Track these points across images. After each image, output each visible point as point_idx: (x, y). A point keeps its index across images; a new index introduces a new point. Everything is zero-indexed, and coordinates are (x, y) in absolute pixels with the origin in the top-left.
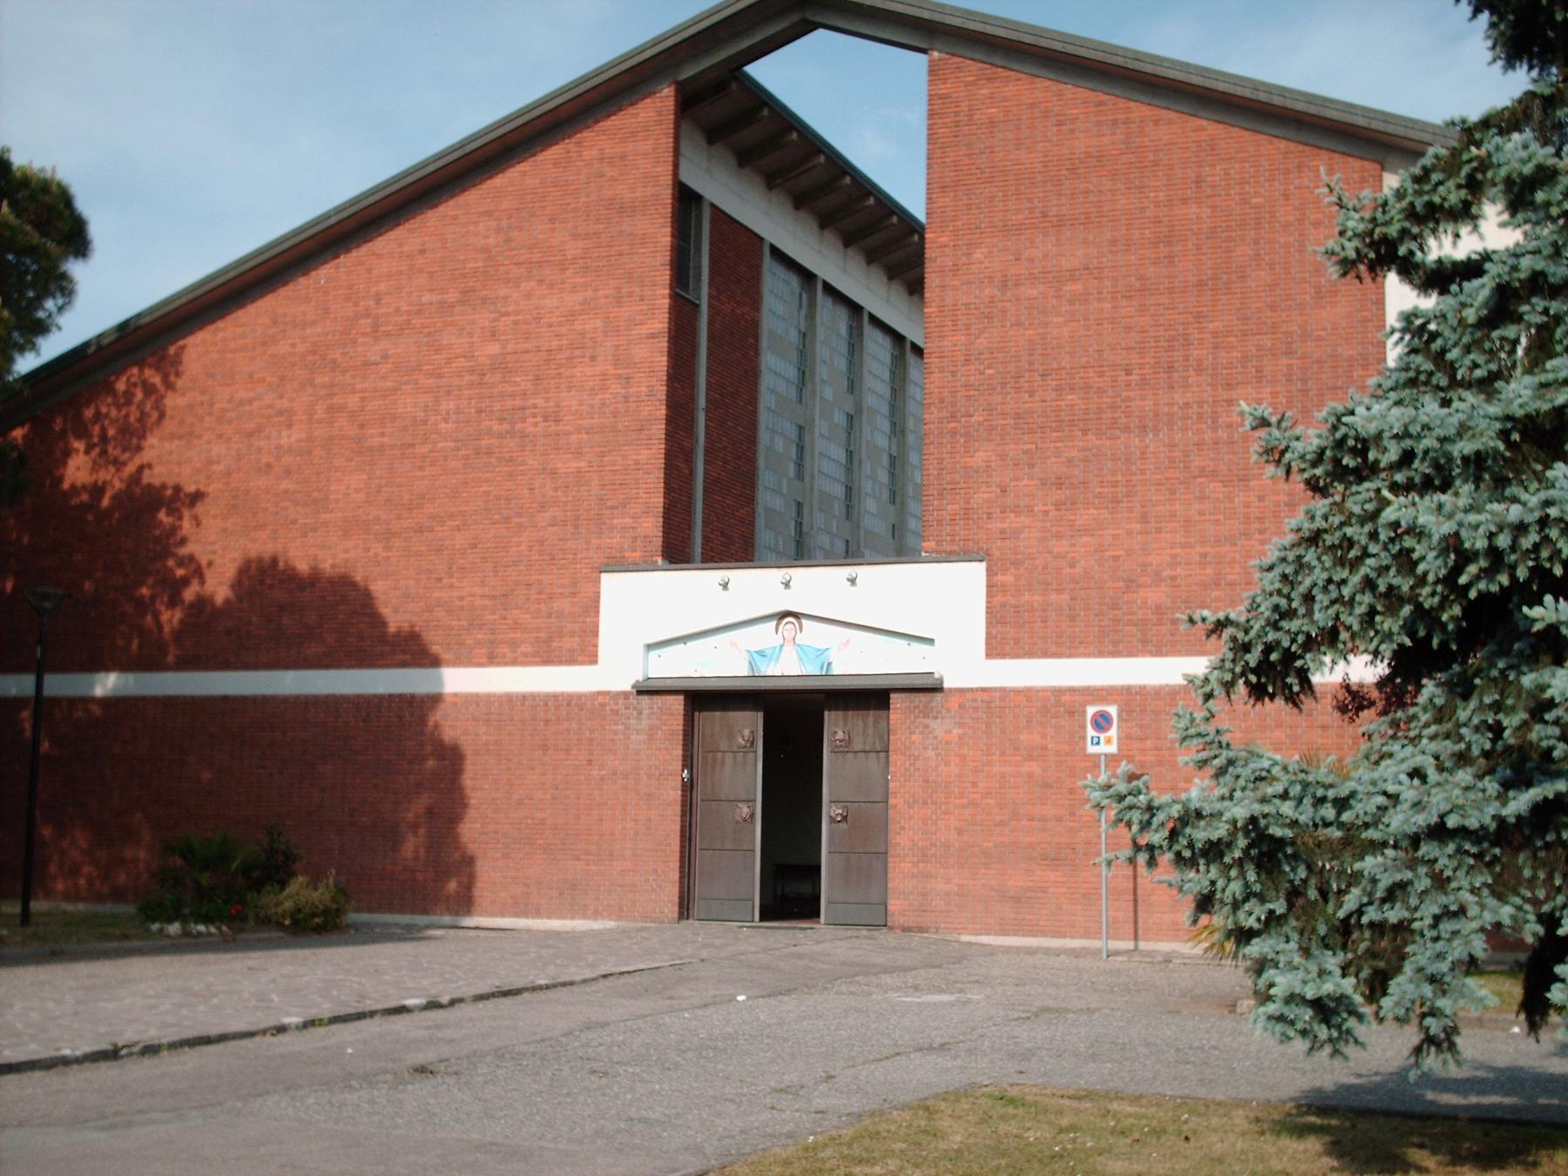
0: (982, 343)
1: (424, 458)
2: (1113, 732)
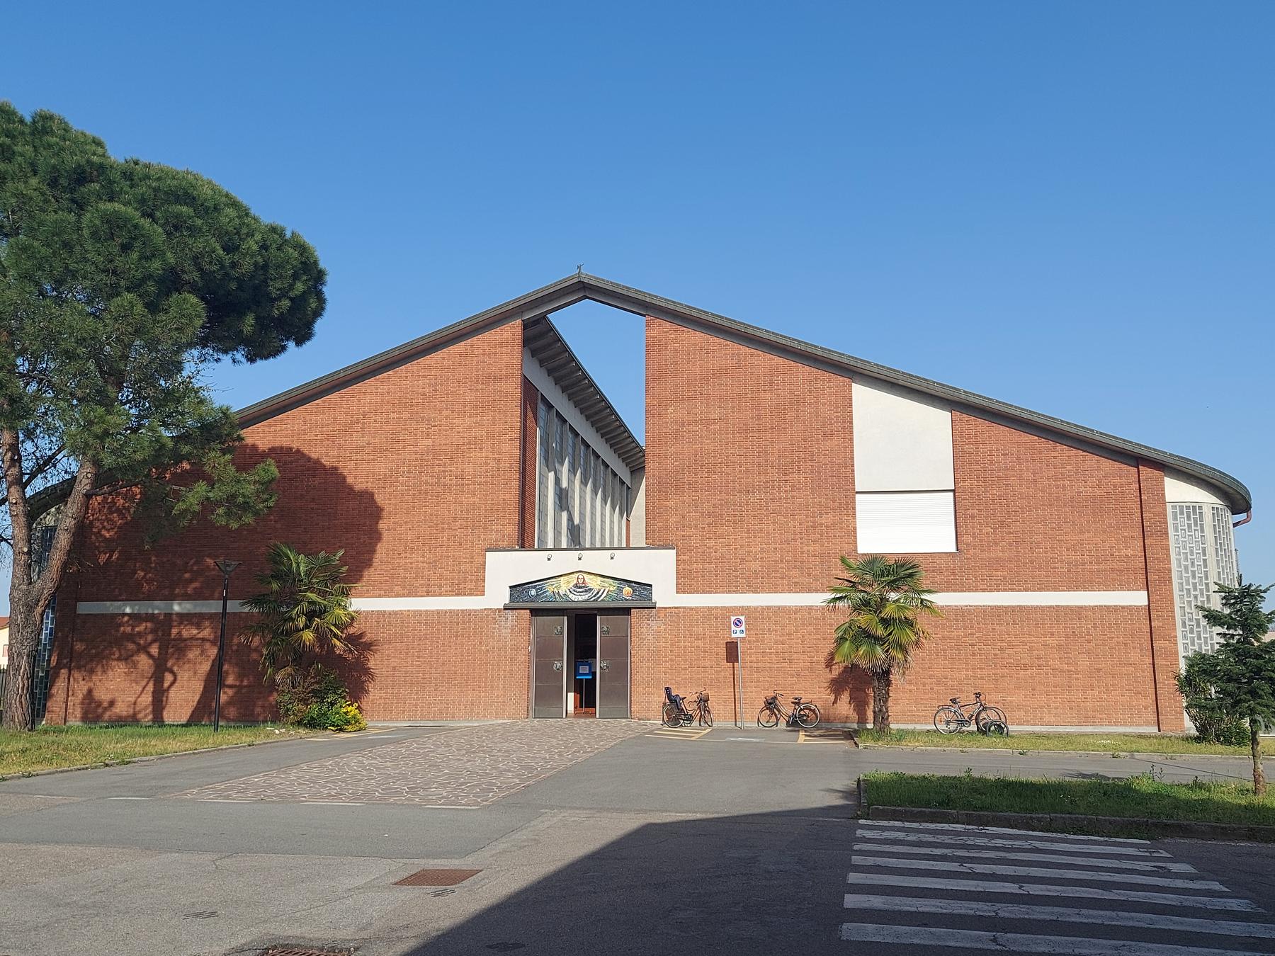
0: (673, 450)
1: (390, 494)
2: (743, 628)
